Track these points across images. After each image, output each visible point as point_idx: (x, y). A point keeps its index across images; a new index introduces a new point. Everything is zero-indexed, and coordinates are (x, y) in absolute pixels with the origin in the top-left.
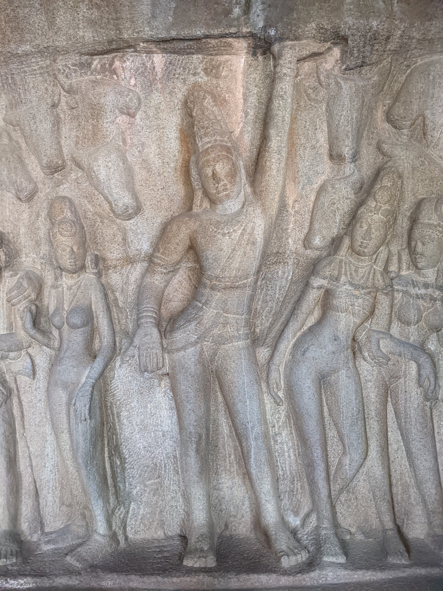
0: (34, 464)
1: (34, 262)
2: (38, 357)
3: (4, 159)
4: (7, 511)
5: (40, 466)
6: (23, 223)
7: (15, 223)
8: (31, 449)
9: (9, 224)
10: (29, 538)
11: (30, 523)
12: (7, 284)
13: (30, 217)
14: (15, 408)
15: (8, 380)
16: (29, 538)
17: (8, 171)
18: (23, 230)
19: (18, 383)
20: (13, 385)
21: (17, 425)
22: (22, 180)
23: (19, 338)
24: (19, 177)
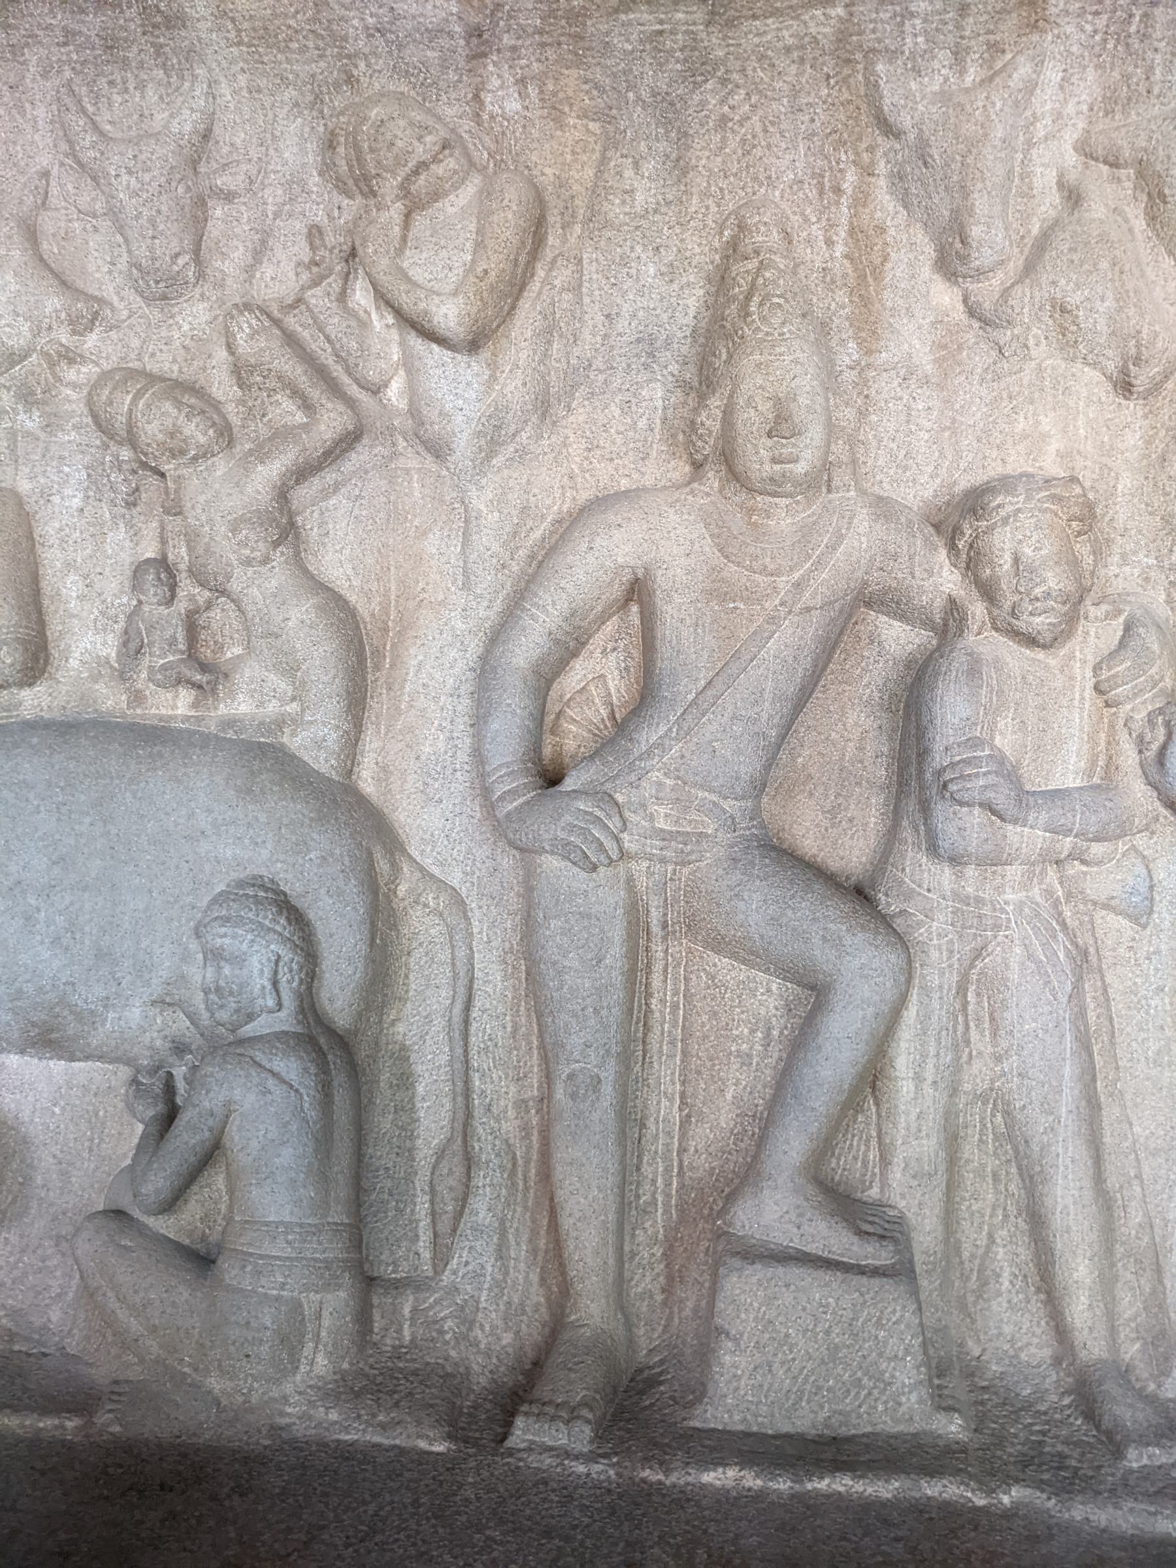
0: (1146, 1171)
1: (1147, 579)
2: (1161, 863)
3: (1104, 265)
4: (1102, 1306)
5: (1161, 1182)
6: (1127, 461)
7: (1104, 460)
8: (1137, 1129)
9: (1088, 463)
10: (1152, 1387)
11: (1145, 1344)
12: (1092, 639)
13: (1148, 443)
14: (1092, 1006)
15: (1068, 921)
16: (1152, 1387)
17: (1118, 301)
18: (1126, 482)
19: (1100, 933)
20: (1084, 939)
21: (1097, 1057)
22: (1157, 328)
23: (1130, 802)
24: (1148, 318)
